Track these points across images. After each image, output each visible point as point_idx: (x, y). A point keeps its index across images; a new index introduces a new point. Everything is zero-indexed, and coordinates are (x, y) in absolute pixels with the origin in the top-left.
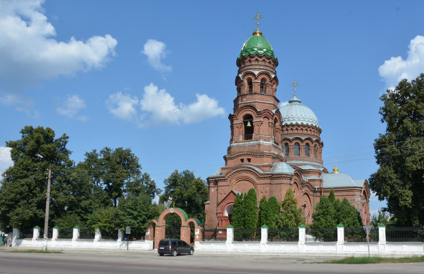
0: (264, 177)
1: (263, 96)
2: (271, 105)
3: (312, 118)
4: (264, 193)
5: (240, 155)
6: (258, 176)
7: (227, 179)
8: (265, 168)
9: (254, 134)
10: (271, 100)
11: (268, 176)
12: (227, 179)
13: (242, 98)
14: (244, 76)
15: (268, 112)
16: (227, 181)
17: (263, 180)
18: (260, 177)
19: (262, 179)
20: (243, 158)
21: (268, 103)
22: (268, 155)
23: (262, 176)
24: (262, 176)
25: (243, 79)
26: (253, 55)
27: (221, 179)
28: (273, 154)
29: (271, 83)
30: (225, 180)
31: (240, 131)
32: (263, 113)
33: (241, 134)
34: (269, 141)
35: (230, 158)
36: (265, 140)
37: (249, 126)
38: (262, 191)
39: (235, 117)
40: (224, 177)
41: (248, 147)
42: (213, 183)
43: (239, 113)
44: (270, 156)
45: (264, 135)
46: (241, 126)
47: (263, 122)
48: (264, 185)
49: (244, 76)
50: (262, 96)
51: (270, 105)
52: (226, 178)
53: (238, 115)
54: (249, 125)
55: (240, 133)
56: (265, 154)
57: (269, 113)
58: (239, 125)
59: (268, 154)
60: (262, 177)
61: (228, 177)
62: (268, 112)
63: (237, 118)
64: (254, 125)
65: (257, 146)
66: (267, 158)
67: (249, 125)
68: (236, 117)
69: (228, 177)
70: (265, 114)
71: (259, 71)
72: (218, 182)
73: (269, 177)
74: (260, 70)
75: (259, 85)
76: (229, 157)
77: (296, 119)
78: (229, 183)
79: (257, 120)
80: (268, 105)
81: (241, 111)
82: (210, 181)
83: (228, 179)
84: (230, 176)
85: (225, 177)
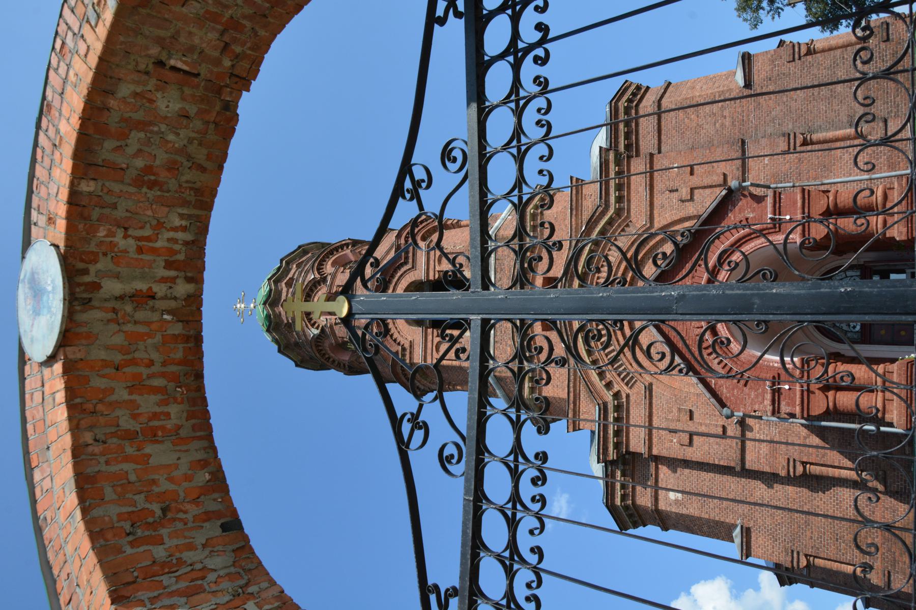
0: (619, 187)
4: (695, 181)
6: (610, 222)
7: (617, 395)
8: (584, 203)
11: (613, 168)
12: (617, 395)
14: (312, 322)
16: (628, 396)
17: (633, 194)
18: (619, 212)
19: (629, 201)
23: (612, 199)
24: (612, 199)
25: (317, 328)
26: (271, 290)
30: (618, 408)
38: (684, 192)
39: (404, 355)
42: (639, 488)
43: (395, 337)
48: (659, 185)
49: (312, 322)
52: (608, 396)
53: (399, 344)
58: (430, 337)
60: (619, 199)
63: (407, 346)
68: (404, 349)
69: (609, 385)
72: (632, 449)
73: (618, 162)
75: (342, 272)
78: (635, 389)
79: (422, 262)
82: (624, 498)
83: (616, 388)
84: (609, 385)
85: (605, 404)
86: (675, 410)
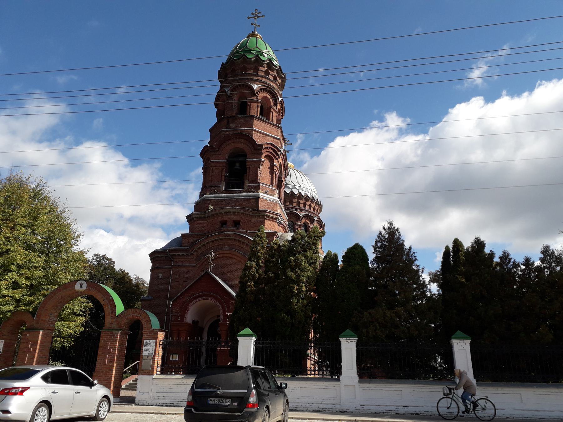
1: (265, 124)
2: (276, 140)
3: (311, 188)
5: (221, 213)
7: (192, 254)
9: (247, 182)
10: (276, 133)
13: (228, 123)
15: (272, 149)
20: (225, 218)
21: (271, 137)
22: (272, 218)
27: (181, 254)
28: (280, 217)
29: (277, 108)
30: (187, 255)
31: (222, 176)
32: (265, 148)
33: (223, 179)
34: (273, 196)
35: (201, 218)
36: (266, 192)
37: (238, 168)
40: (186, 250)
41: (235, 201)
44: (276, 219)
45: (265, 184)
46: (223, 168)
47: (264, 162)
50: (262, 123)
51: (274, 140)
54: (237, 166)
55: (221, 178)
56: (268, 214)
57: (274, 151)
59: (272, 215)
61: (196, 251)
62: (272, 149)
64: (247, 166)
65: (253, 200)
66: (269, 222)
67: (237, 166)
70: (267, 150)
71: (259, 85)
74: (261, 84)
76: (198, 216)
77: (290, 186)
80: (272, 139)
81: (225, 142)
86: (187, 276)
